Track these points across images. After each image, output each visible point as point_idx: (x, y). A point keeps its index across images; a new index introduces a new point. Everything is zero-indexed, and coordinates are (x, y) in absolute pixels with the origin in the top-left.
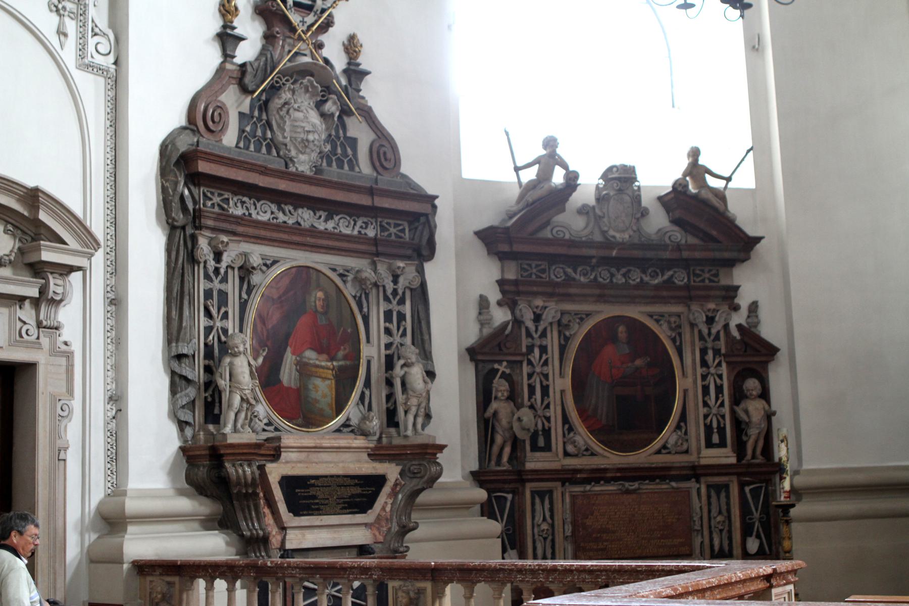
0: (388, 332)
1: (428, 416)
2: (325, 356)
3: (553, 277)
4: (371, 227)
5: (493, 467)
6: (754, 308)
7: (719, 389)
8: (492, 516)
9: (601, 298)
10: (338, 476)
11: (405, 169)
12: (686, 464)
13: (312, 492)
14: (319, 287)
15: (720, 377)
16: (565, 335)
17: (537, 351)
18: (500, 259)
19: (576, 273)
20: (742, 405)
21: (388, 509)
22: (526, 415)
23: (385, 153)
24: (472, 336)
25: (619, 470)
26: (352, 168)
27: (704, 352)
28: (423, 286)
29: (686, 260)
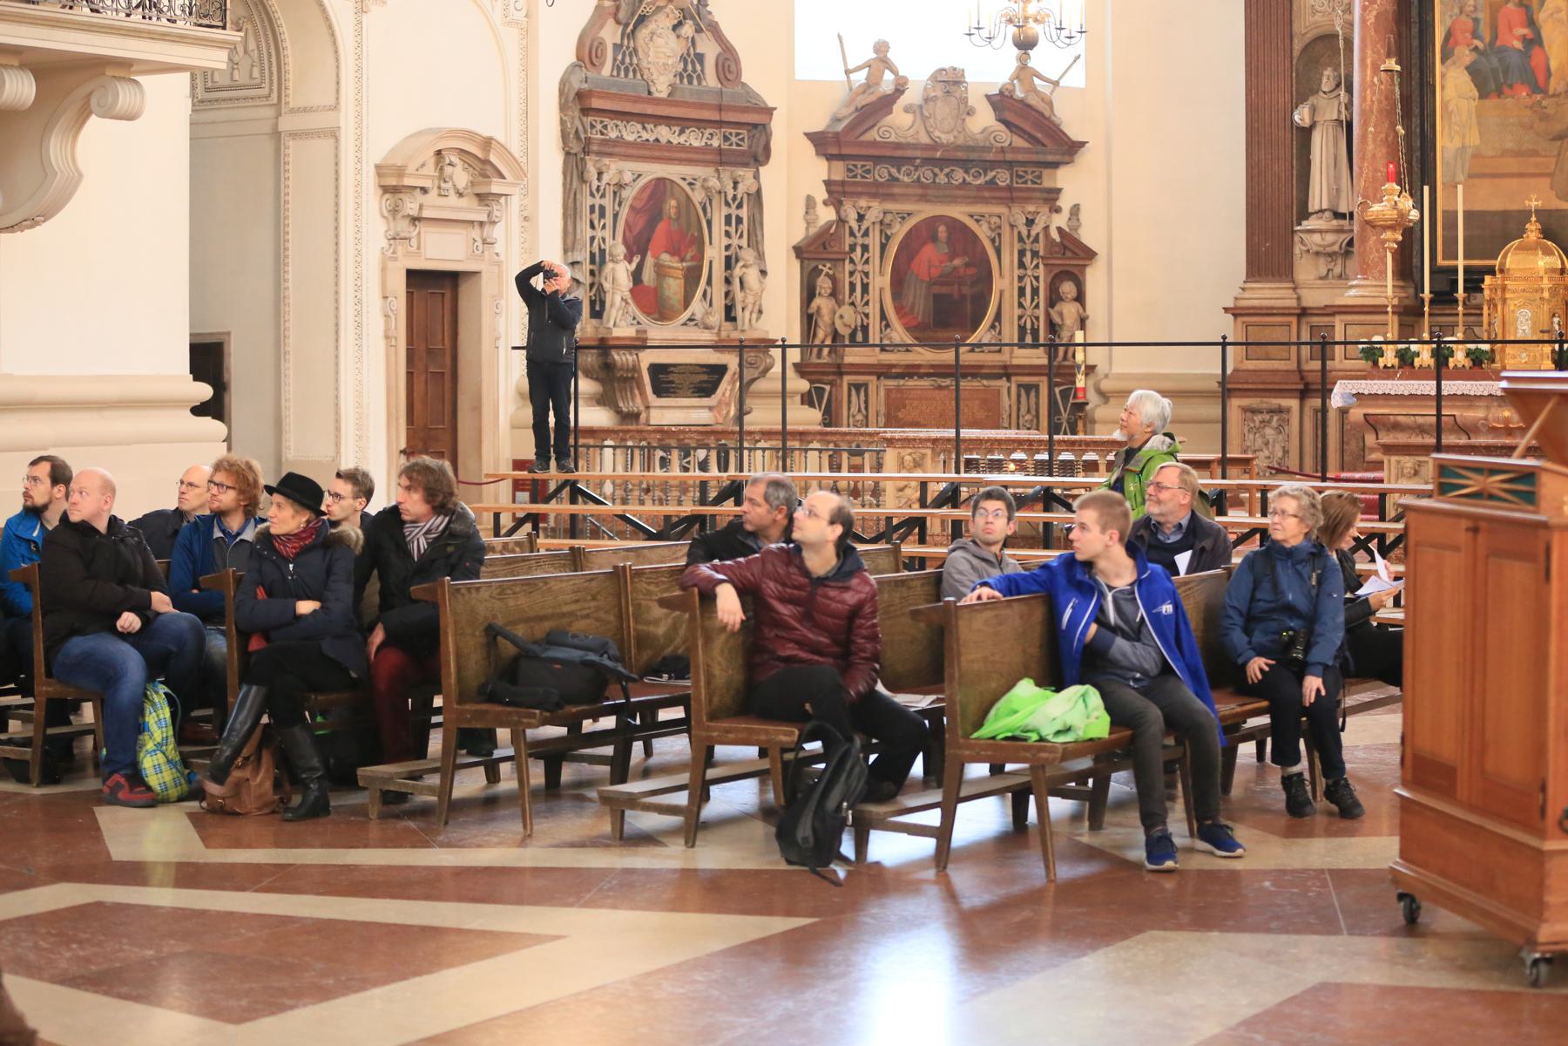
0: (728, 234)
1: (760, 312)
2: (676, 258)
3: (877, 177)
4: (715, 138)
5: (814, 360)
6: (1075, 210)
7: (1035, 291)
8: (812, 405)
9: (924, 198)
10: (691, 365)
11: (746, 78)
12: (998, 364)
13: (671, 377)
14: (673, 196)
15: (1037, 279)
16: (886, 234)
17: (859, 249)
18: (828, 159)
19: (899, 172)
20: (1057, 308)
21: (727, 394)
22: (847, 311)
23: (729, 66)
24: (799, 234)
25: (932, 366)
26: (700, 83)
27: (1022, 253)
28: (759, 192)
29: (1010, 162)
